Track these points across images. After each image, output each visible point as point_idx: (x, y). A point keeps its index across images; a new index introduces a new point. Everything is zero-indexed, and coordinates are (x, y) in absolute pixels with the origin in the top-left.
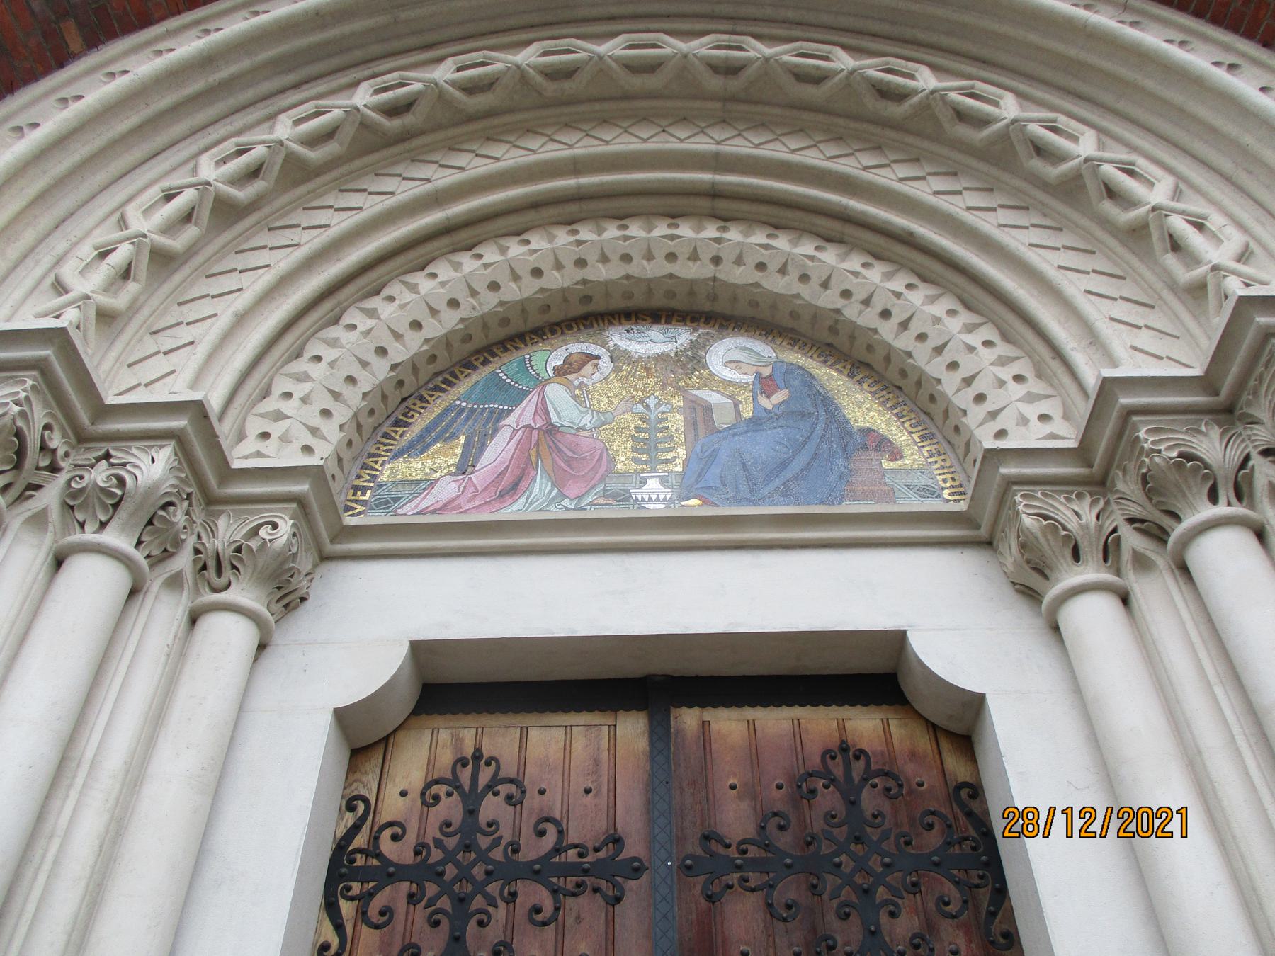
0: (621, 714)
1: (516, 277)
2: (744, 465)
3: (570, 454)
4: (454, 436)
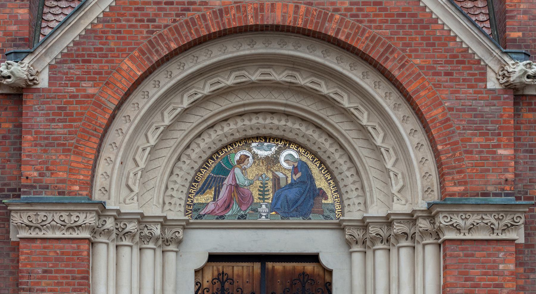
0: (255, 263)
1: (226, 136)
2: (287, 201)
3: (242, 195)
4: (211, 188)
